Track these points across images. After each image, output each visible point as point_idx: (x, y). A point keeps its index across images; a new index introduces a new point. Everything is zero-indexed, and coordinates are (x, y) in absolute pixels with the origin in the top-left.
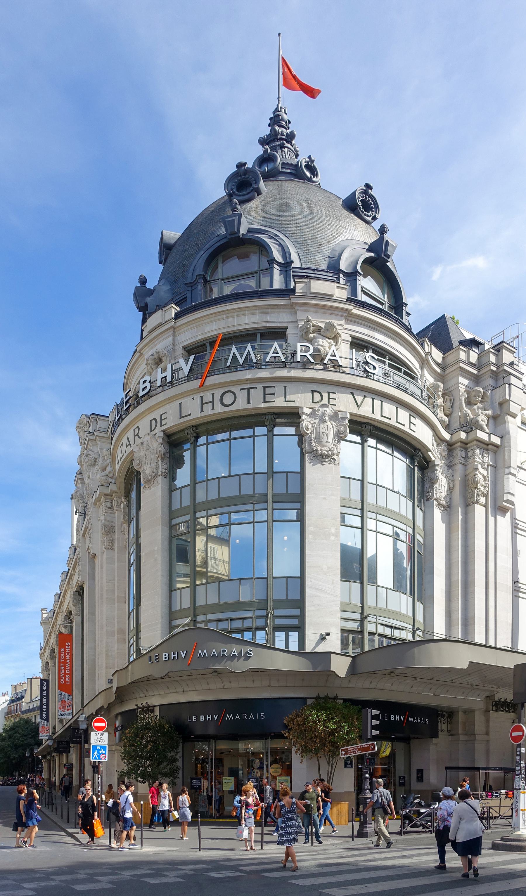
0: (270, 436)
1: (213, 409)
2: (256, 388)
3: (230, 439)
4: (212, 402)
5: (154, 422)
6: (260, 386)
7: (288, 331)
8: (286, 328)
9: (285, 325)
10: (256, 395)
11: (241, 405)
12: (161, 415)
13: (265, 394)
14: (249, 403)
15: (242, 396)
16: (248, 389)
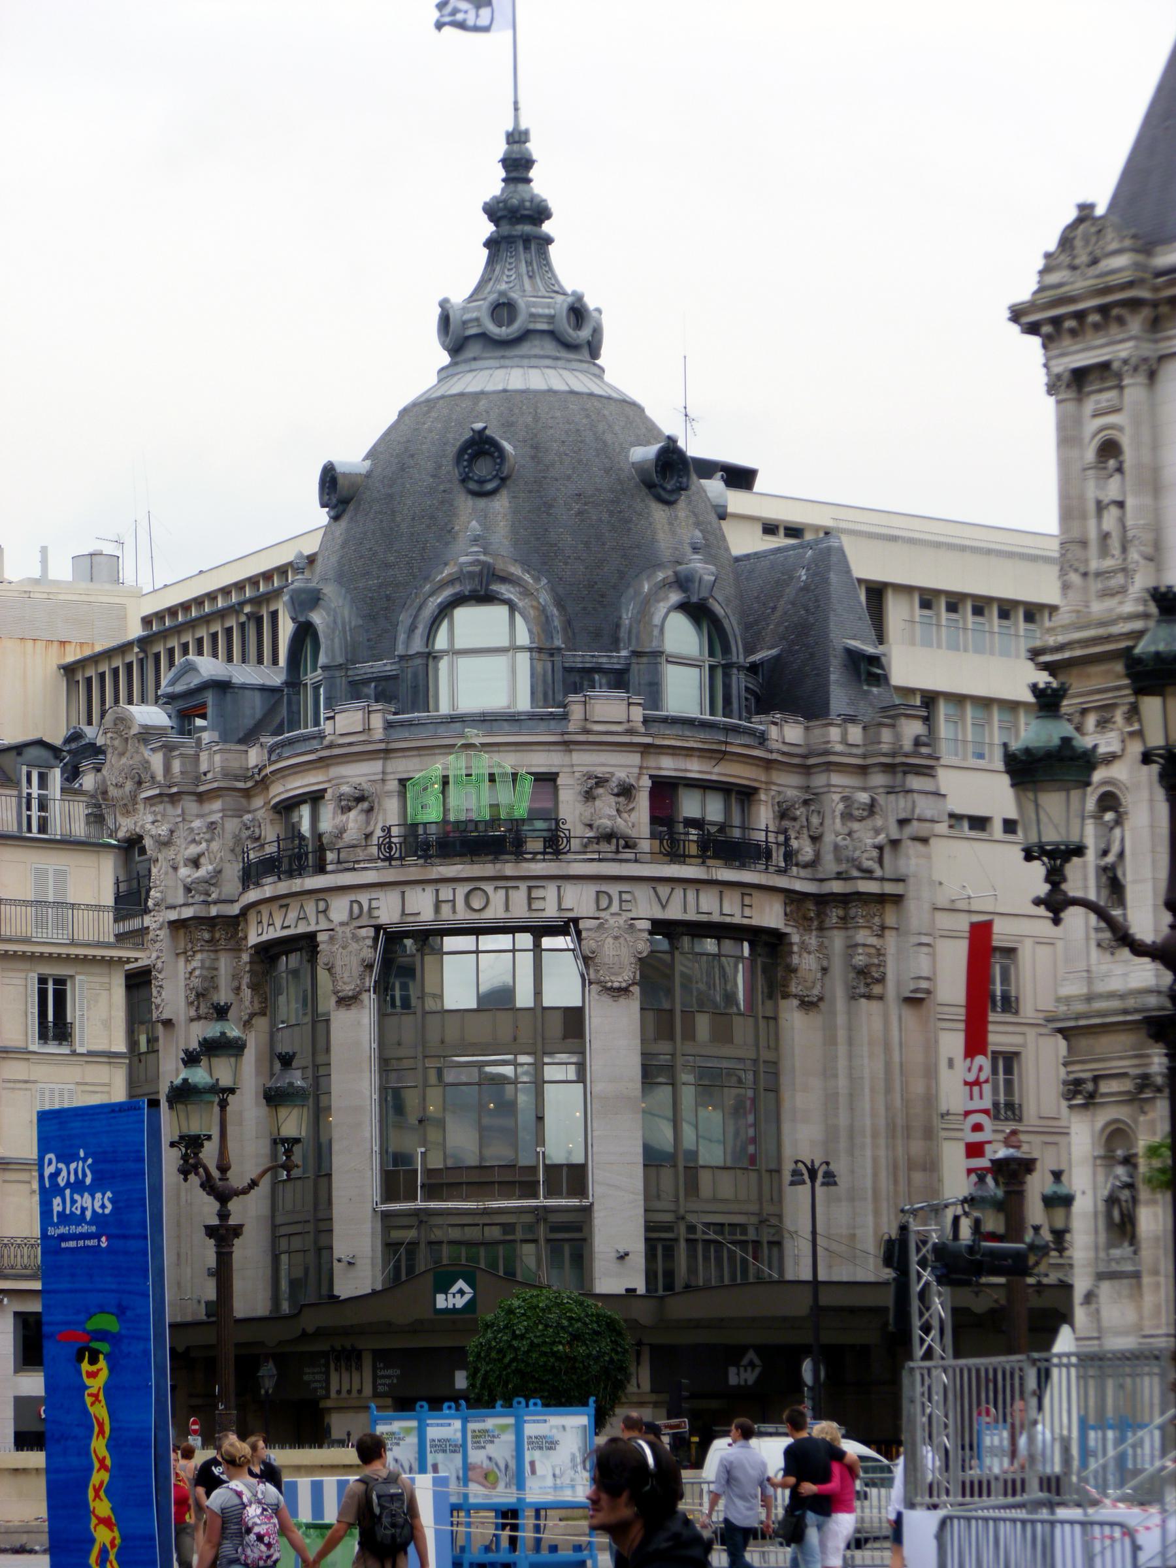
0: (537, 948)
1: (454, 912)
2: (517, 887)
3: (477, 952)
4: (453, 901)
5: (355, 906)
6: (523, 886)
7: (560, 781)
8: (557, 774)
9: (554, 770)
10: (519, 896)
11: (495, 911)
12: (370, 900)
13: (530, 899)
14: (507, 909)
15: (497, 898)
16: (507, 888)
